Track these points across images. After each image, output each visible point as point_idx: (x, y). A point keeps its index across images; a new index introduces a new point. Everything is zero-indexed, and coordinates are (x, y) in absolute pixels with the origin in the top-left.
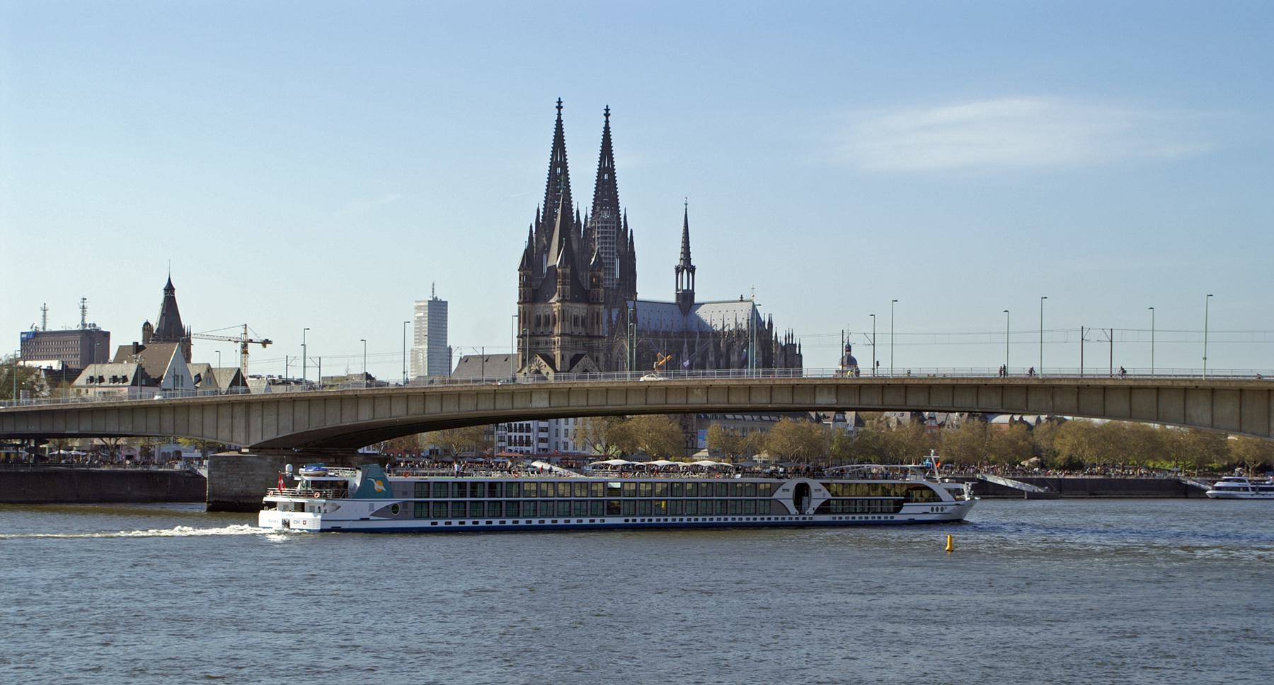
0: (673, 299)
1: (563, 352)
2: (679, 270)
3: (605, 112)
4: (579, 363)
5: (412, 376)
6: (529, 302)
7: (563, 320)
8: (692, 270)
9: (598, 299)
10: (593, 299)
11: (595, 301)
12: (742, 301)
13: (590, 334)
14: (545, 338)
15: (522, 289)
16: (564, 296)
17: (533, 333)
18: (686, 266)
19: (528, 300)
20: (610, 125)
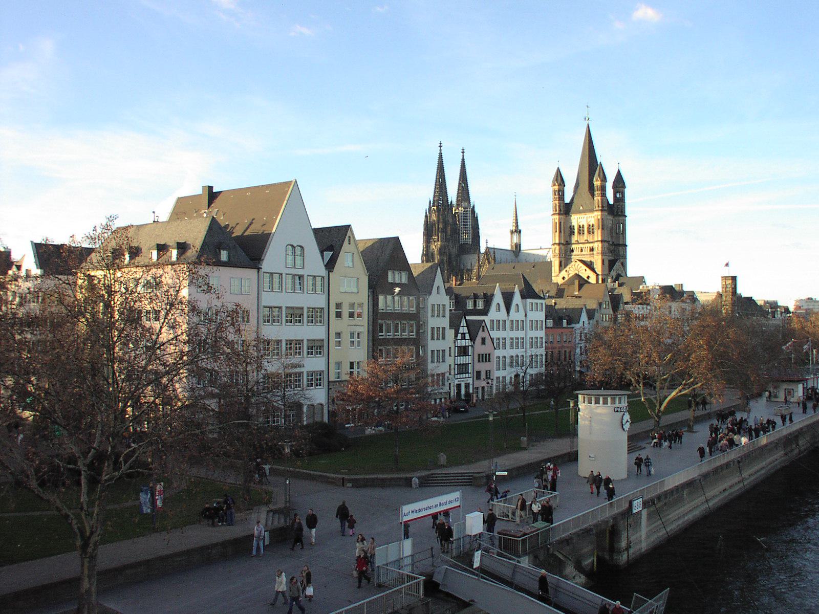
0: (509, 248)
1: (604, 257)
2: (512, 232)
3: (462, 151)
4: (614, 268)
5: (578, 265)
6: (562, 214)
7: (603, 229)
8: (520, 231)
9: (622, 212)
10: (617, 212)
11: (620, 213)
12: (541, 249)
13: (615, 243)
14: (581, 246)
15: (557, 202)
16: (602, 207)
17: (567, 242)
18: (517, 231)
19: (562, 212)
20: (465, 158)
